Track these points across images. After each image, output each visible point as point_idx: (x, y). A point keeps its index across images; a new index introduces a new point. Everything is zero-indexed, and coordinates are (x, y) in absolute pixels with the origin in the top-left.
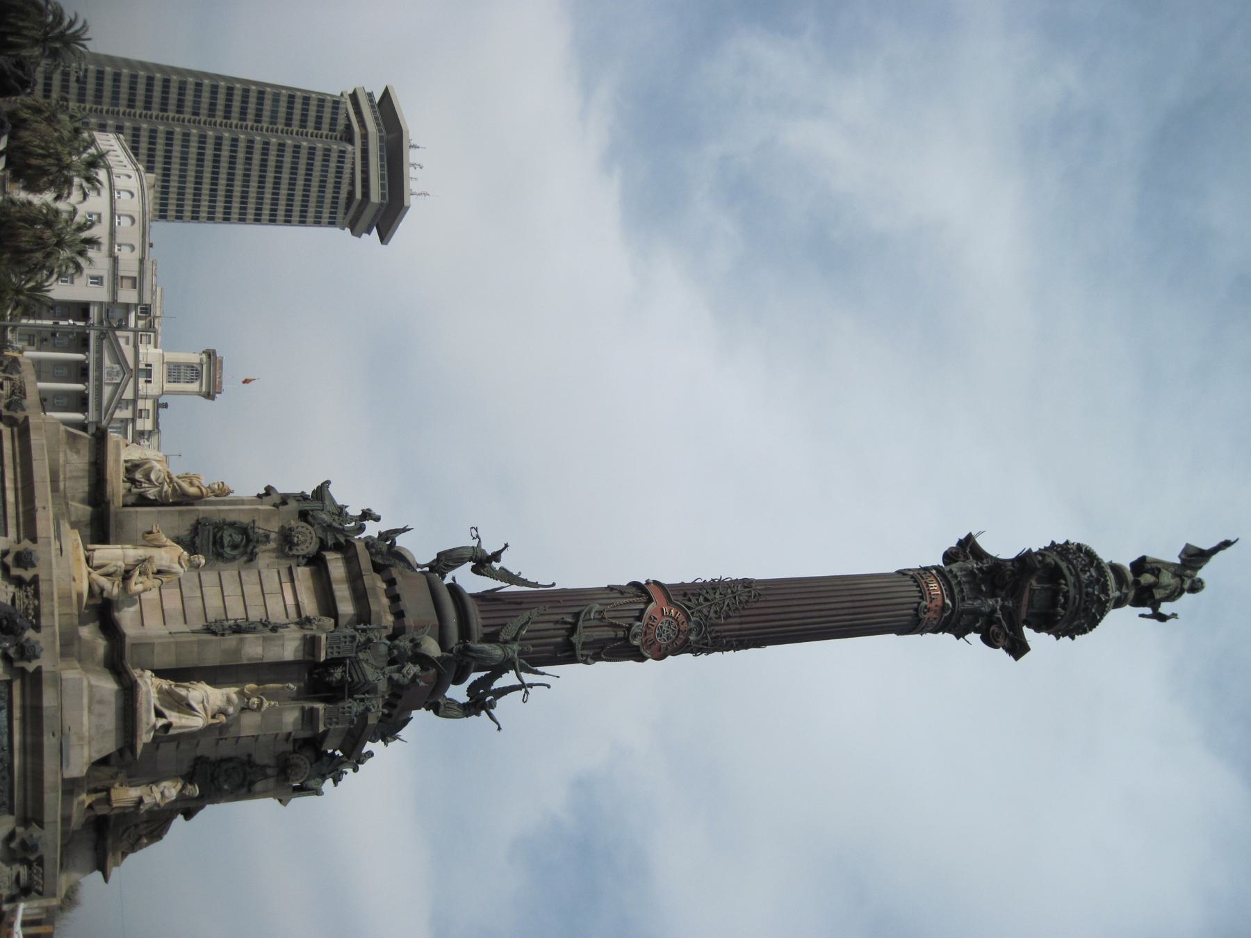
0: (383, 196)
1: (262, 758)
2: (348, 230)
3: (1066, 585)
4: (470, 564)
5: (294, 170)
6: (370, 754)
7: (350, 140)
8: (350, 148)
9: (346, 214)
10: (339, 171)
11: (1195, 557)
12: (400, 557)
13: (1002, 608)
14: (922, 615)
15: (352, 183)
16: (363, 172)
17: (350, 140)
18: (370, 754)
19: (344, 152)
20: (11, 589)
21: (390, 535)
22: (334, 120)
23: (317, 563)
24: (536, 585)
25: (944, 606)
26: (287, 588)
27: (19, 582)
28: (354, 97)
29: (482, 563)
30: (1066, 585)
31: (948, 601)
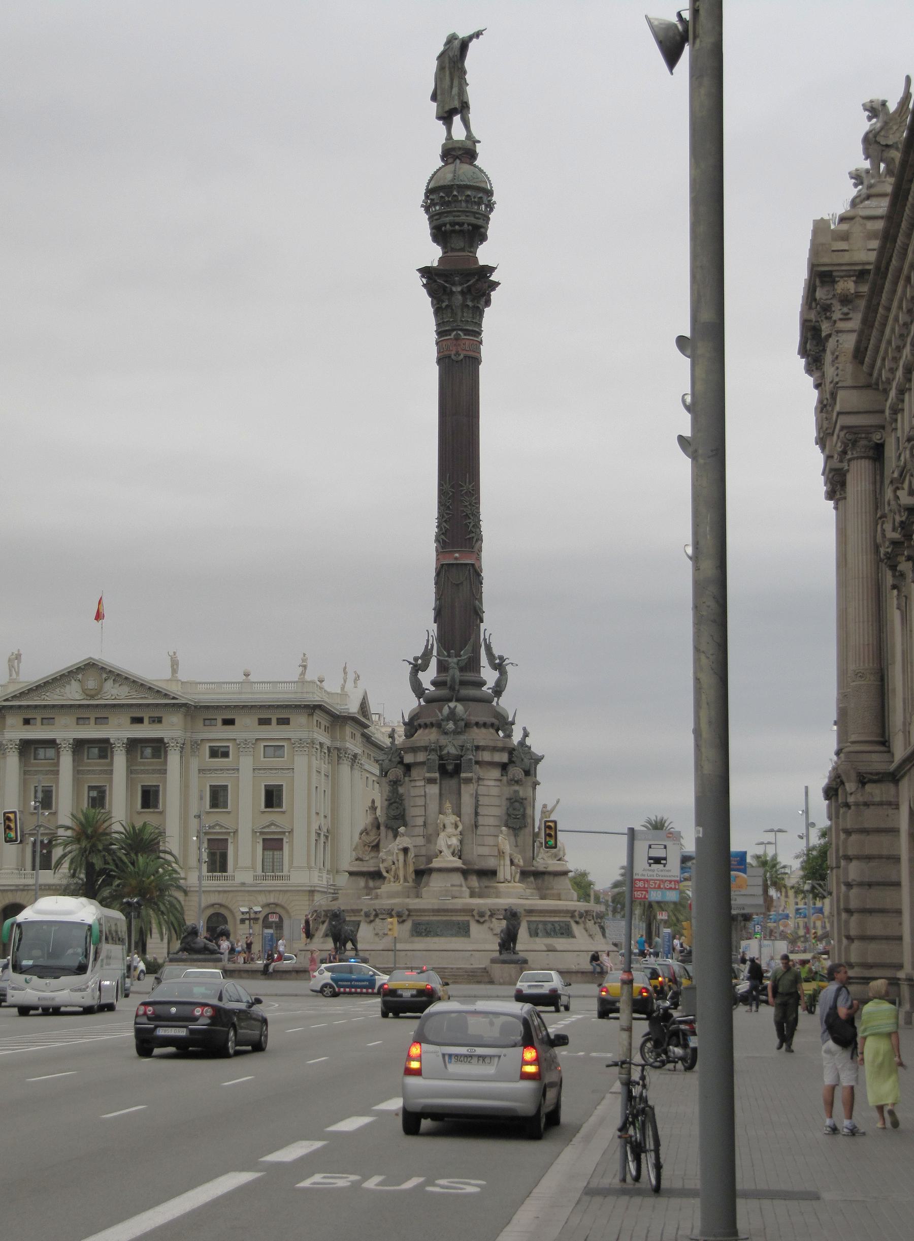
1: (508, 791)
3: (445, 225)
4: (421, 675)
6: (524, 729)
12: (413, 718)
13: (461, 284)
14: (462, 357)
18: (524, 729)
20: (377, 920)
21: (405, 724)
23: (408, 768)
24: (428, 641)
25: (457, 338)
26: (418, 784)
27: (376, 915)
29: (418, 667)
30: (445, 225)
31: (452, 336)
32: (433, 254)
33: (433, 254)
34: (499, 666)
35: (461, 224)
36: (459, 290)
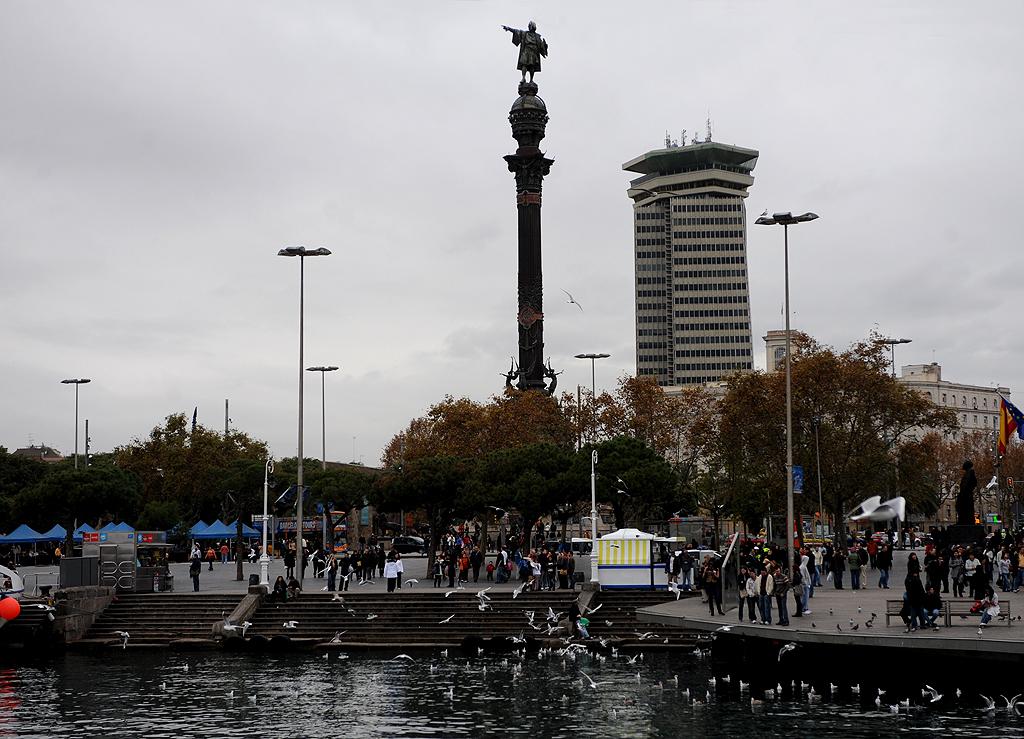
0: (709, 167)
2: (749, 189)
4: (512, 382)
5: (697, 248)
7: (667, 200)
8: (674, 202)
9: (734, 196)
10: (693, 208)
11: (518, 37)
15: (702, 195)
16: (692, 187)
17: (667, 200)
19: (675, 207)
22: (653, 216)
28: (636, 198)
29: (510, 378)
32: (512, 147)
33: (512, 147)
34: (552, 375)
35: (526, 130)
36: (529, 167)
